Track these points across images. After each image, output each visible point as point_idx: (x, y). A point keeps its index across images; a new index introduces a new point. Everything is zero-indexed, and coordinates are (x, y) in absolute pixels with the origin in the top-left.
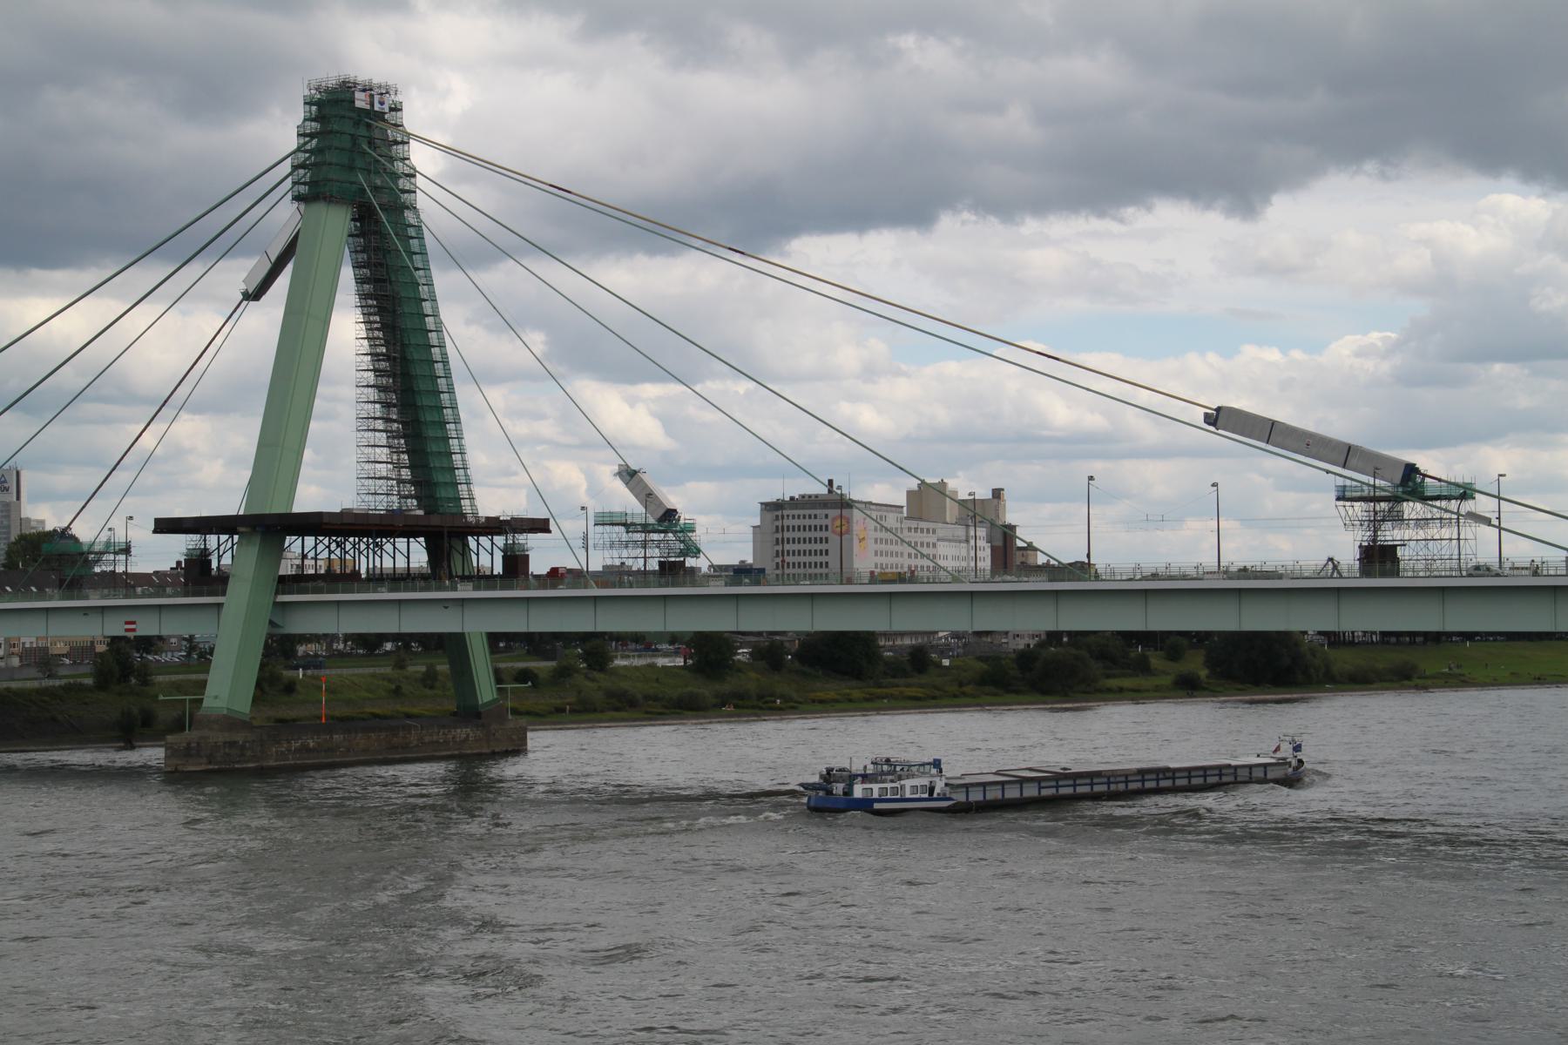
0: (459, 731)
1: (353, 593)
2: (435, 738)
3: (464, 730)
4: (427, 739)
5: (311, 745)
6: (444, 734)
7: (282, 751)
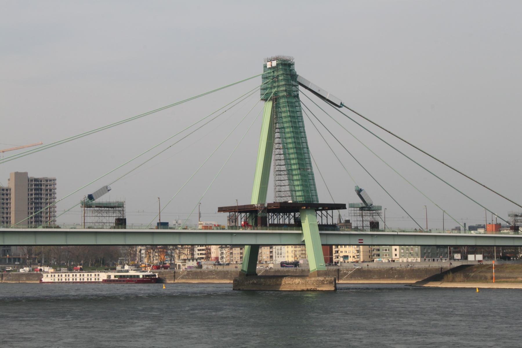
0: (296, 280)
1: (282, 230)
2: (289, 282)
3: (298, 280)
4: (287, 282)
5: (255, 282)
6: (292, 281)
7: (248, 284)
